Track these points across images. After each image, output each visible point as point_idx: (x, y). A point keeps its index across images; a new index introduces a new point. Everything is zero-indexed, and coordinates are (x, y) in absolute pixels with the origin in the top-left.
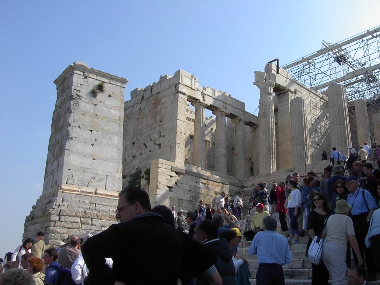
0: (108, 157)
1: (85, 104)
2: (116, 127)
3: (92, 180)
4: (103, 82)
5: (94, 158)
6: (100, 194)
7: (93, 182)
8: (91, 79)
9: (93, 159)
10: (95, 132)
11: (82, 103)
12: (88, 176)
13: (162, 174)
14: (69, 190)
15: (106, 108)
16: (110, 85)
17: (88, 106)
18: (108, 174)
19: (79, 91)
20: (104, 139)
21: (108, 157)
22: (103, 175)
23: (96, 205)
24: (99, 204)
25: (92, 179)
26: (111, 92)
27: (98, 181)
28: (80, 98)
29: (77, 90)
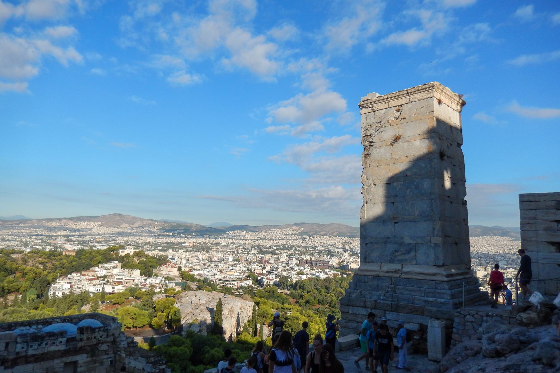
0: (416, 215)
1: (378, 150)
2: (424, 165)
3: (397, 254)
4: (399, 106)
5: (397, 221)
6: (406, 273)
7: (398, 256)
8: (383, 111)
9: (395, 223)
10: (395, 184)
11: (374, 150)
12: (391, 248)
13: (531, 222)
14: (367, 270)
15: (406, 144)
16: (410, 105)
17: (382, 150)
18: (419, 241)
19: (370, 135)
20: (408, 191)
21: (416, 215)
22: (410, 244)
23: (396, 290)
24: (398, 289)
25: (396, 251)
26: (413, 115)
27: (402, 254)
28: (372, 144)
29: (368, 136)
